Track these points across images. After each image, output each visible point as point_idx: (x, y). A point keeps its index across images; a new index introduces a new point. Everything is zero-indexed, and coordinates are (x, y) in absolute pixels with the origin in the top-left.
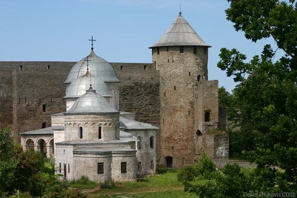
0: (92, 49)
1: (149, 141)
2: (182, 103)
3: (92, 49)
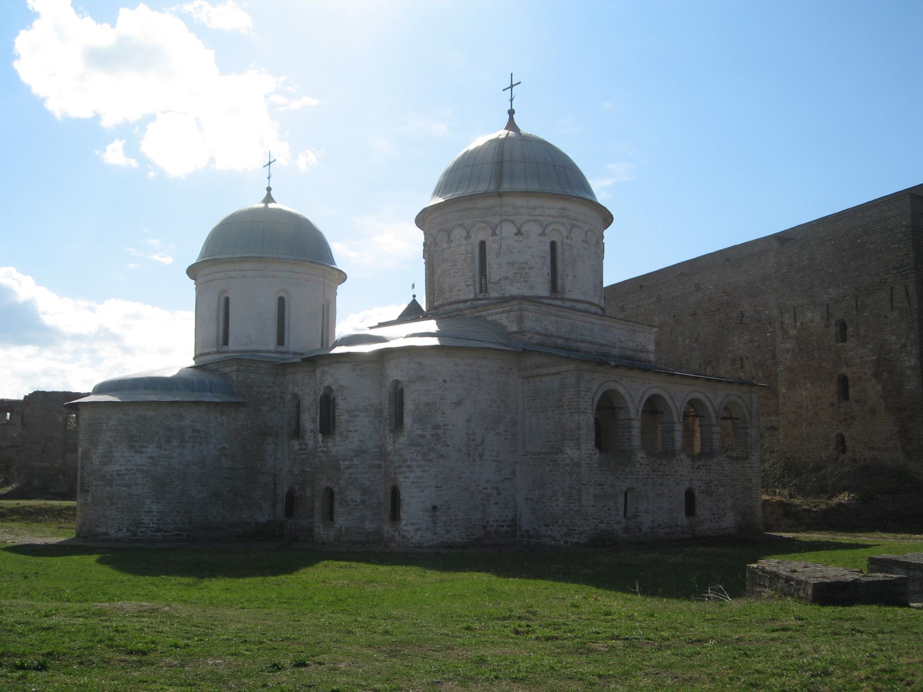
0: (511, 112)
3: (511, 112)
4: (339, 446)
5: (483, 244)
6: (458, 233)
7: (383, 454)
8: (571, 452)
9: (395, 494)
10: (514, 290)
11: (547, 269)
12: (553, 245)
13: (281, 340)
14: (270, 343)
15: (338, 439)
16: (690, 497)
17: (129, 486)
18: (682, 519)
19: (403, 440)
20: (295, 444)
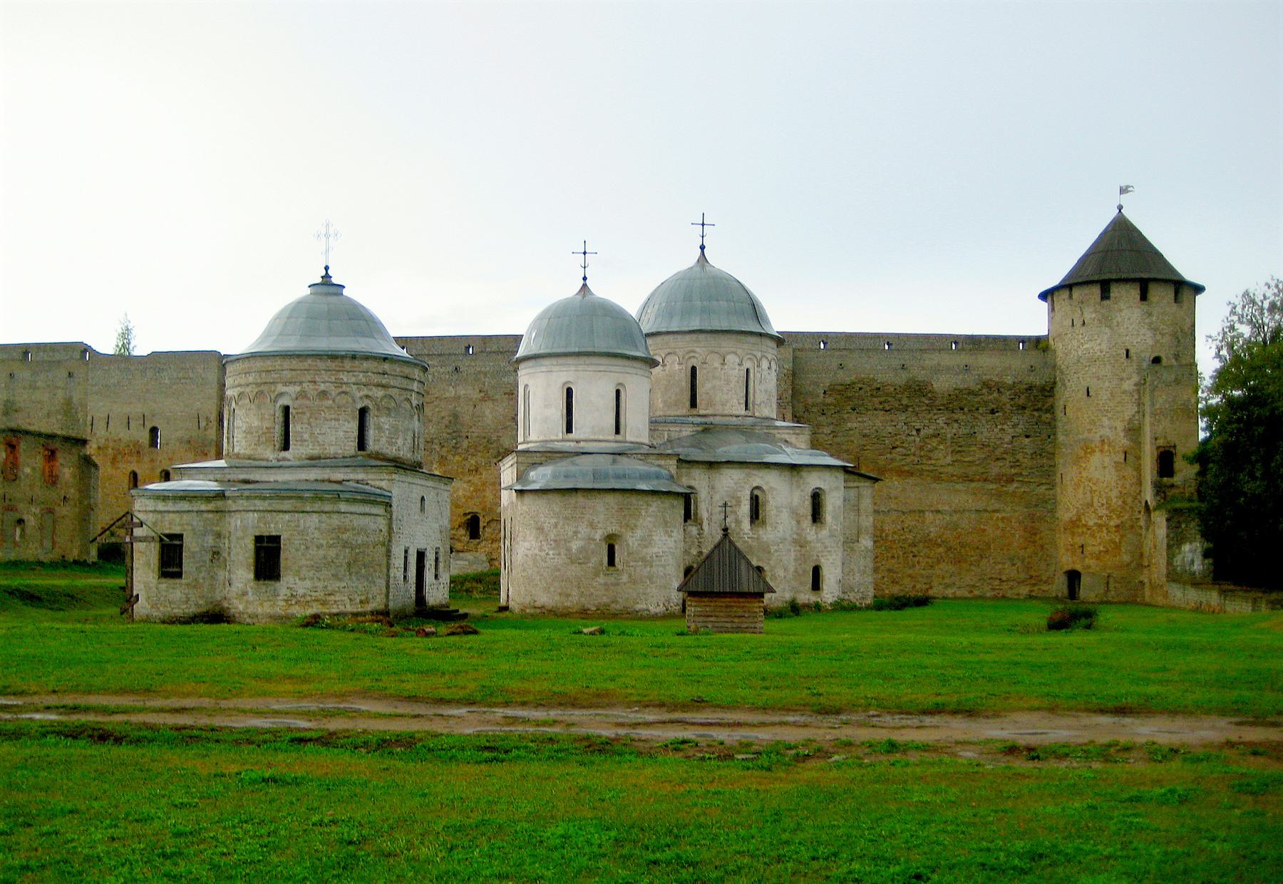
0: (702, 248)
1: (808, 503)
2: (1106, 432)
3: (702, 248)
4: (768, 534)
6: (731, 358)
9: (816, 571)
15: (769, 528)
17: (664, 566)
19: (824, 533)
20: (694, 530)
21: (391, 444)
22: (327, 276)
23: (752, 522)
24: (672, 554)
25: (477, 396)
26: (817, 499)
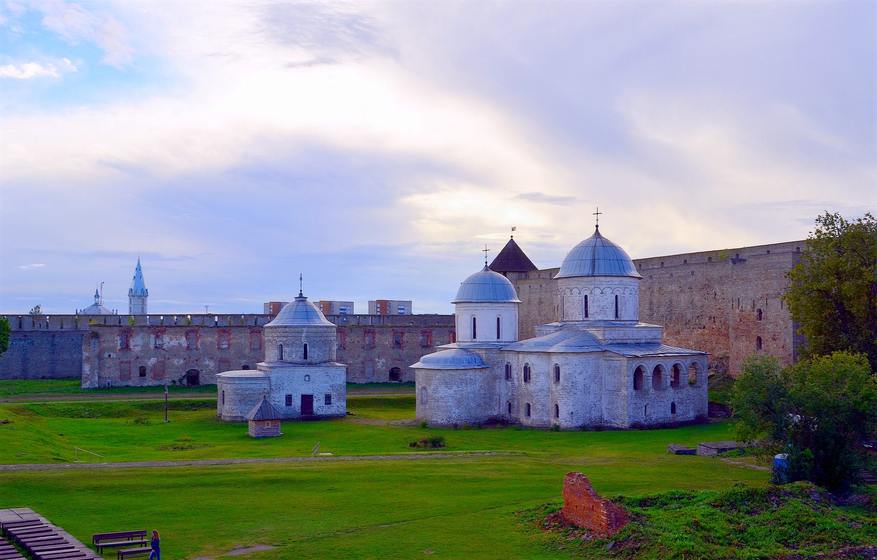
0: (597, 226)
3: (597, 226)
4: (532, 387)
5: (586, 297)
6: (575, 291)
7: (549, 390)
8: (624, 392)
9: (557, 406)
10: (599, 318)
11: (614, 308)
12: (616, 297)
13: (498, 337)
14: (494, 338)
16: (673, 405)
18: (670, 415)
19: (559, 387)
21: (289, 356)
22: (301, 294)
23: (526, 380)
24: (453, 397)
25: (679, 290)
26: (557, 370)
